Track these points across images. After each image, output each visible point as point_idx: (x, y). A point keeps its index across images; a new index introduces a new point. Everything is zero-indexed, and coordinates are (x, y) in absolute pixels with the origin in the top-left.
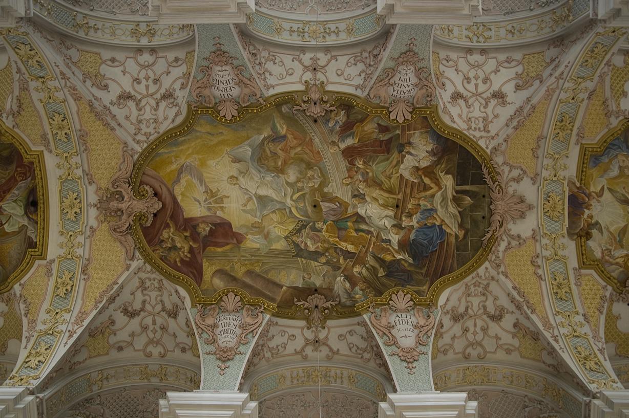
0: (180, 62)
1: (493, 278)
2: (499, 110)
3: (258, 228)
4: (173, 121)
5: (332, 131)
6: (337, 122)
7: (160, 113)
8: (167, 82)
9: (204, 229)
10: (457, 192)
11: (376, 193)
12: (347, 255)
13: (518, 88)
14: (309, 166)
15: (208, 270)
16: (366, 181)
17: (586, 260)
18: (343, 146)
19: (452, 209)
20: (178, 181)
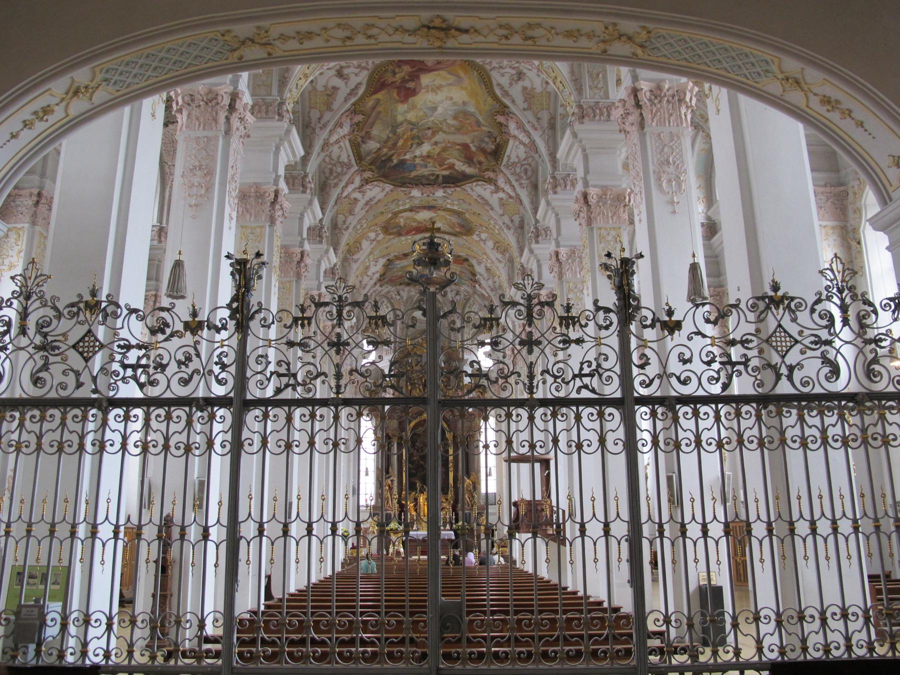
0: (544, 85)
1: (384, 189)
2: (488, 191)
3: (414, 107)
4: (499, 85)
5: (482, 141)
6: (487, 143)
7: (508, 70)
8: (531, 74)
9: (411, 85)
10: (438, 176)
11: (438, 150)
12: (395, 144)
13: (501, 199)
14: (456, 129)
15: (379, 96)
16: (446, 147)
17: (396, 214)
18: (471, 145)
19: (426, 173)
20: (450, 74)
